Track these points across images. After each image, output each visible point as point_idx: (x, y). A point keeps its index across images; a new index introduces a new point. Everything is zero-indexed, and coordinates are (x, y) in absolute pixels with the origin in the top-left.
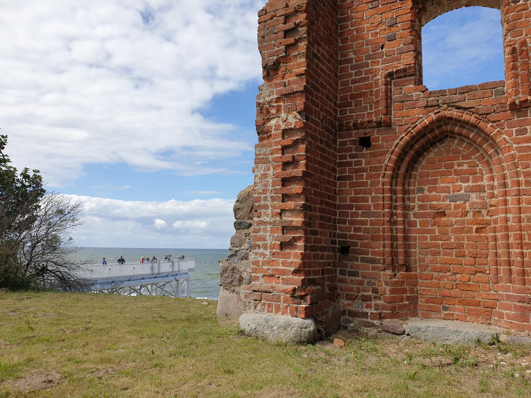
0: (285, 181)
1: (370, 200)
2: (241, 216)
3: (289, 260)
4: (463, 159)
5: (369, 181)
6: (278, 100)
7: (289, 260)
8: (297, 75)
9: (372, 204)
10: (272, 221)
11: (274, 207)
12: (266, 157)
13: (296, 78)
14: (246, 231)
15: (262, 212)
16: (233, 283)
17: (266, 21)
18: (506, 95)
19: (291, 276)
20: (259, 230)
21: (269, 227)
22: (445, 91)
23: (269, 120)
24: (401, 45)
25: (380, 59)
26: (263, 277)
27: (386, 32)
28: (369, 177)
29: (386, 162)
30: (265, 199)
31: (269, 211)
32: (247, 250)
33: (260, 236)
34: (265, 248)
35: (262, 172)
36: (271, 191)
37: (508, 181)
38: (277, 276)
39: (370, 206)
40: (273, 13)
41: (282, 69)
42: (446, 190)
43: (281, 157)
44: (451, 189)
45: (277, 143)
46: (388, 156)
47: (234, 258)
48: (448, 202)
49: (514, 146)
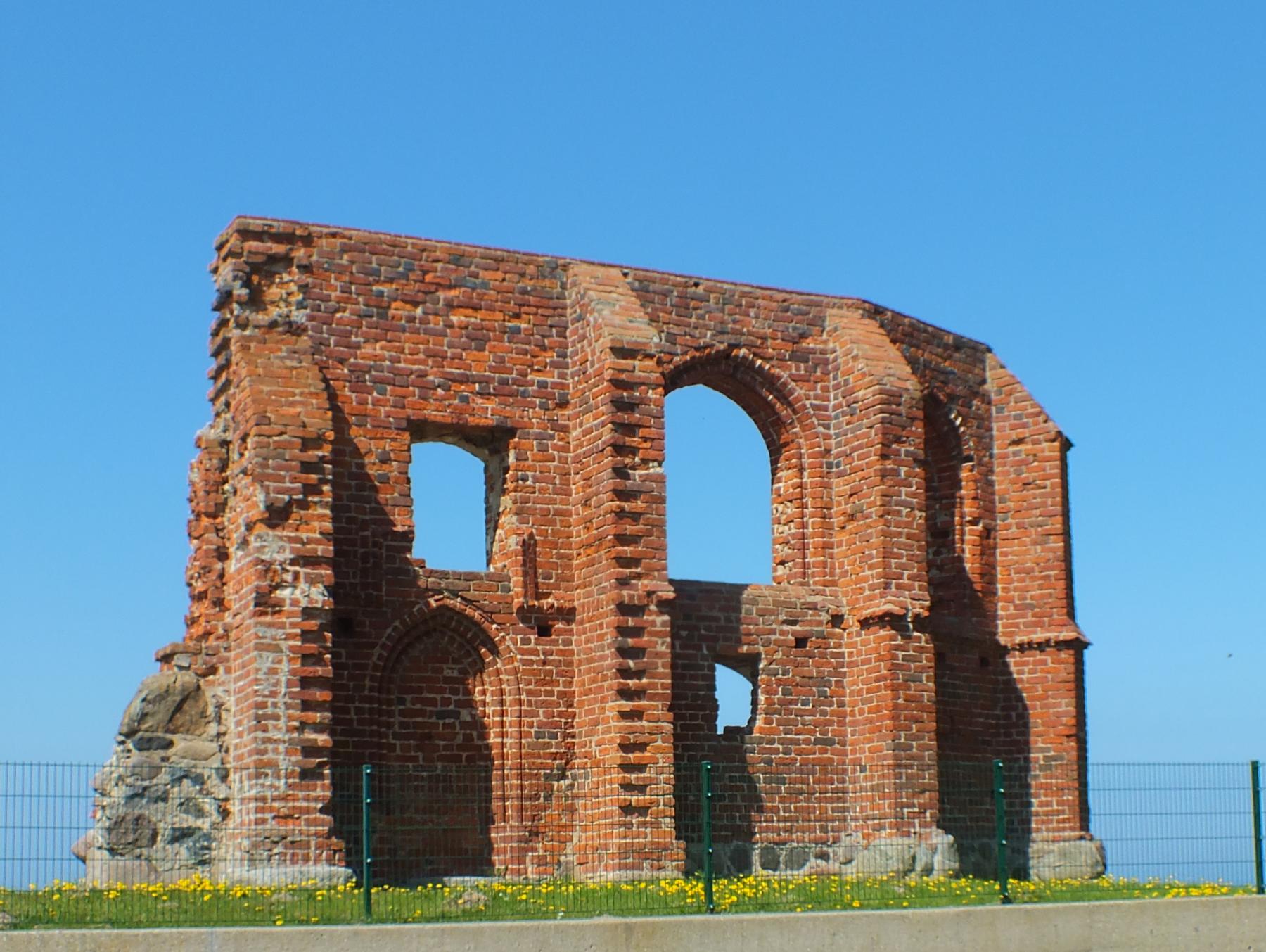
0: (305, 682)
1: (352, 712)
2: (151, 727)
3: (313, 794)
4: (453, 663)
5: (352, 684)
6: (293, 562)
7: (313, 794)
8: (321, 533)
9: (355, 717)
10: (286, 737)
11: (290, 718)
12: (274, 642)
13: (318, 536)
14: (162, 753)
15: (270, 727)
16: (139, 843)
17: (269, 436)
18: (511, 593)
19: (318, 815)
20: (265, 752)
21: (281, 748)
22: (447, 573)
23: (279, 586)
24: (396, 495)
25: (368, 506)
26: (274, 818)
27: (375, 467)
28: (351, 677)
29: (375, 658)
30: (275, 705)
31: (282, 723)
32: (166, 785)
33: (269, 759)
34: (279, 778)
35: (269, 664)
36: (285, 695)
37: (508, 698)
38: (296, 816)
39: (351, 720)
40: (281, 428)
41: (294, 516)
42: (433, 702)
43: (300, 647)
44: (439, 703)
45: (293, 625)
46: (377, 650)
47: (137, 799)
48: (433, 720)
49: (519, 657)
